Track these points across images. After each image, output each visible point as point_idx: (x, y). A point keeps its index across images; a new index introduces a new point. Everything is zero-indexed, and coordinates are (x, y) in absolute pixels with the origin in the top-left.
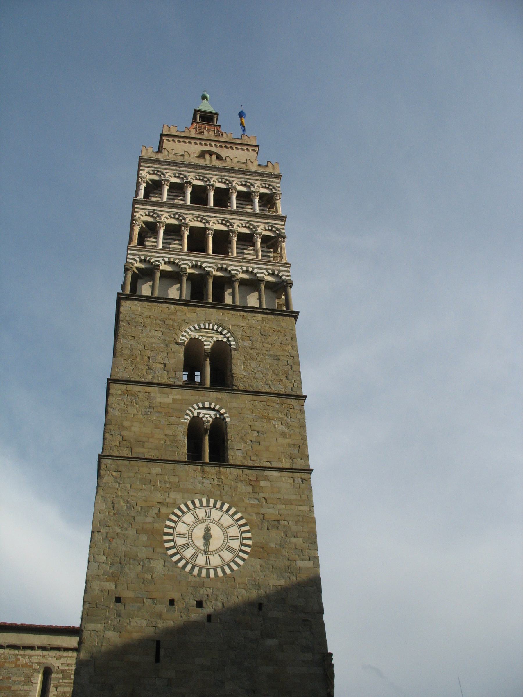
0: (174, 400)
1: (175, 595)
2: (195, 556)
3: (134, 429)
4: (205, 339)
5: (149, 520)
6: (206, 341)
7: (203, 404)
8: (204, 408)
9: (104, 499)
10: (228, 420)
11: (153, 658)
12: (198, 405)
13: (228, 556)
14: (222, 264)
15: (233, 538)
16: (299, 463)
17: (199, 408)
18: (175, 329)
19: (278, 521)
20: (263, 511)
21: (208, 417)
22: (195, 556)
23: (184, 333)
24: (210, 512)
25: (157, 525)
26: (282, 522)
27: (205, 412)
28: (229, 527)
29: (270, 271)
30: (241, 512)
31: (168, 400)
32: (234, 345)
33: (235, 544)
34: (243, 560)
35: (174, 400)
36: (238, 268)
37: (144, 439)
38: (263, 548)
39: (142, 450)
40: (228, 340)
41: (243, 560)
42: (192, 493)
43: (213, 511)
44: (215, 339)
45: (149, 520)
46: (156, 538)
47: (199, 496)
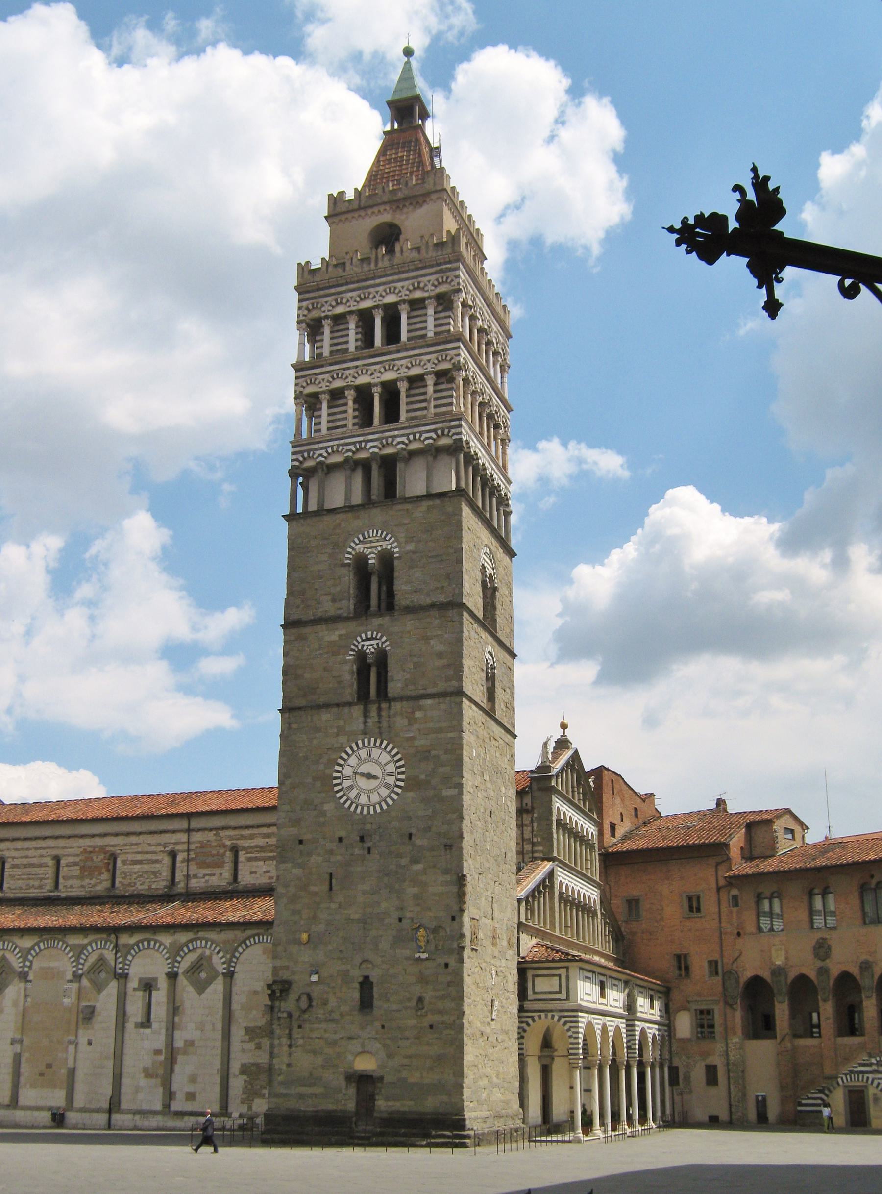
1: (342, 834)
2: (358, 796)
3: (307, 676)
4: (370, 550)
5: (321, 767)
6: (370, 554)
7: (366, 635)
8: (367, 639)
11: (326, 887)
12: (361, 637)
15: (390, 774)
17: (363, 640)
21: (370, 647)
22: (358, 796)
23: (349, 550)
24: (371, 751)
25: (328, 771)
26: (433, 753)
27: (368, 643)
28: (386, 764)
31: (334, 637)
32: (397, 552)
34: (397, 794)
35: (340, 636)
40: (392, 547)
42: (352, 737)
45: (321, 767)
46: (327, 782)
47: (362, 736)
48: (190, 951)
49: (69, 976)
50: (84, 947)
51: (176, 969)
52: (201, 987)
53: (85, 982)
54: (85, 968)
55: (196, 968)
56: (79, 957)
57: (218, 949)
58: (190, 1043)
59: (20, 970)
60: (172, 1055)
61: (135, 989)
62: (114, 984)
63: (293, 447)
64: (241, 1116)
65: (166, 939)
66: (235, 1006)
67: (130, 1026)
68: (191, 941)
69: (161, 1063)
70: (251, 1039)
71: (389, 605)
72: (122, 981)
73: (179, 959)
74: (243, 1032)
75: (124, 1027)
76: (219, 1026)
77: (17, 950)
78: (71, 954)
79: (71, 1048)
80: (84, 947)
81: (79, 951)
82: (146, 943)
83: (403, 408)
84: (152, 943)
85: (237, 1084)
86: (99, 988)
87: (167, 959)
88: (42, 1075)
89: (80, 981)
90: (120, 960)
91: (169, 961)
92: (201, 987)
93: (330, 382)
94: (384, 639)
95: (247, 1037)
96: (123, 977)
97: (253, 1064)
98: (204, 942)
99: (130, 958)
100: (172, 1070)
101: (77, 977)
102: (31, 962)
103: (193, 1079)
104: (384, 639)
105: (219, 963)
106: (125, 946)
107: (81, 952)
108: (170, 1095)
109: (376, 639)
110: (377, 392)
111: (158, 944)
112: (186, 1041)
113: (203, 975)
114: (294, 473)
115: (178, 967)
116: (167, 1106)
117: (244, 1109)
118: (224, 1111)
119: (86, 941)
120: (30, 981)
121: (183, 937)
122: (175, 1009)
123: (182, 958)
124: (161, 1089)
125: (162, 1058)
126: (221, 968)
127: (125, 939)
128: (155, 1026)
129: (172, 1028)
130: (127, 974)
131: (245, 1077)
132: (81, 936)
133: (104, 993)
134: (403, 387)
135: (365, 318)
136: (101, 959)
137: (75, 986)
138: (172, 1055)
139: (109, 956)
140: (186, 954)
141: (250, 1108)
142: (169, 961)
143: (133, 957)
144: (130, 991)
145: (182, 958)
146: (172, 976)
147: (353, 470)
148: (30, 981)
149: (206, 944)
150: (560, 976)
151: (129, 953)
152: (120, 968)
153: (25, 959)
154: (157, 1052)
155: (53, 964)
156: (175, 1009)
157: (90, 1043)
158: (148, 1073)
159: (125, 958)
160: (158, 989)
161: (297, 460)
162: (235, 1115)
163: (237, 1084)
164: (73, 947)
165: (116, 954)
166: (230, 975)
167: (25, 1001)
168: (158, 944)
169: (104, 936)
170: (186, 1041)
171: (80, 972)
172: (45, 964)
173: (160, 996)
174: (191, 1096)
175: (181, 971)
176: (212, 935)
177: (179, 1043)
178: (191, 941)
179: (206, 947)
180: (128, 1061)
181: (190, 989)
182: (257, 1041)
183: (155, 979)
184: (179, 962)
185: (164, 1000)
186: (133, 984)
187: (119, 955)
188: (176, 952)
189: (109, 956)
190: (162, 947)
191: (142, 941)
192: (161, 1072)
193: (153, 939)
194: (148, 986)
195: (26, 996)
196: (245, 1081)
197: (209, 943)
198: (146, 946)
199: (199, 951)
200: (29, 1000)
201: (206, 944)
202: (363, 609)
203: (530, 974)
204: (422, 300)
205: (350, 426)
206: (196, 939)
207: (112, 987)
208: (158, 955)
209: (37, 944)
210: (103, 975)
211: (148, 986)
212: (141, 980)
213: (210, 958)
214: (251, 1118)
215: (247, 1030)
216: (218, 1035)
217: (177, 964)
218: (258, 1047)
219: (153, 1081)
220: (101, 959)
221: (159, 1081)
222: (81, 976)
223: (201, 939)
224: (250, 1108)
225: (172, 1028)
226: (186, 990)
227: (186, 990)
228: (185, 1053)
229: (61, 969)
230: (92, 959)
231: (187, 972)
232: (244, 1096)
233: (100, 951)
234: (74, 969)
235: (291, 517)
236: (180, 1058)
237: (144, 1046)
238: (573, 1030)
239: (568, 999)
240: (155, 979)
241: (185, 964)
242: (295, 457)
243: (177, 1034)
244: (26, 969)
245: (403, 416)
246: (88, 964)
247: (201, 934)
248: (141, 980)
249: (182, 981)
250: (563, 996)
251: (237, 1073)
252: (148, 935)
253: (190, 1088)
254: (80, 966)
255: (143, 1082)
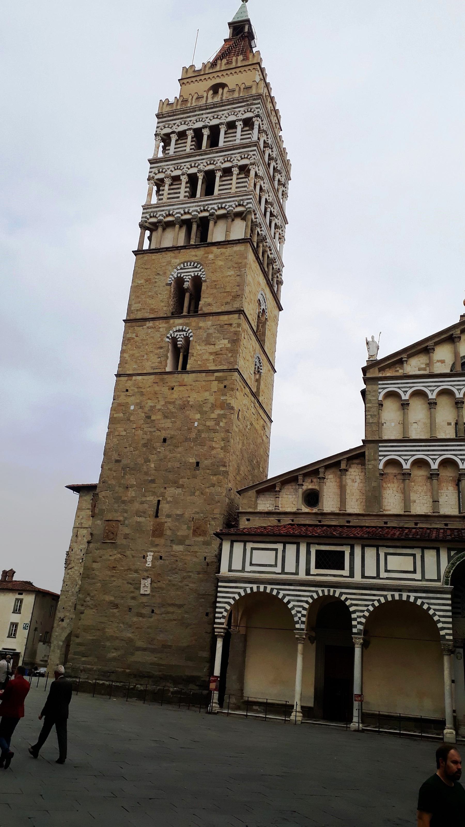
63: (144, 209)
71: (194, 311)
83: (217, 188)
93: (172, 171)
94: (190, 331)
104: (190, 331)
109: (185, 331)
110: (201, 177)
114: (143, 227)
134: (218, 174)
135: (198, 133)
147: (181, 227)
161: (146, 217)
202: (177, 312)
204: (234, 122)
205: (182, 197)
235: (138, 253)
242: (144, 215)
245: (216, 192)
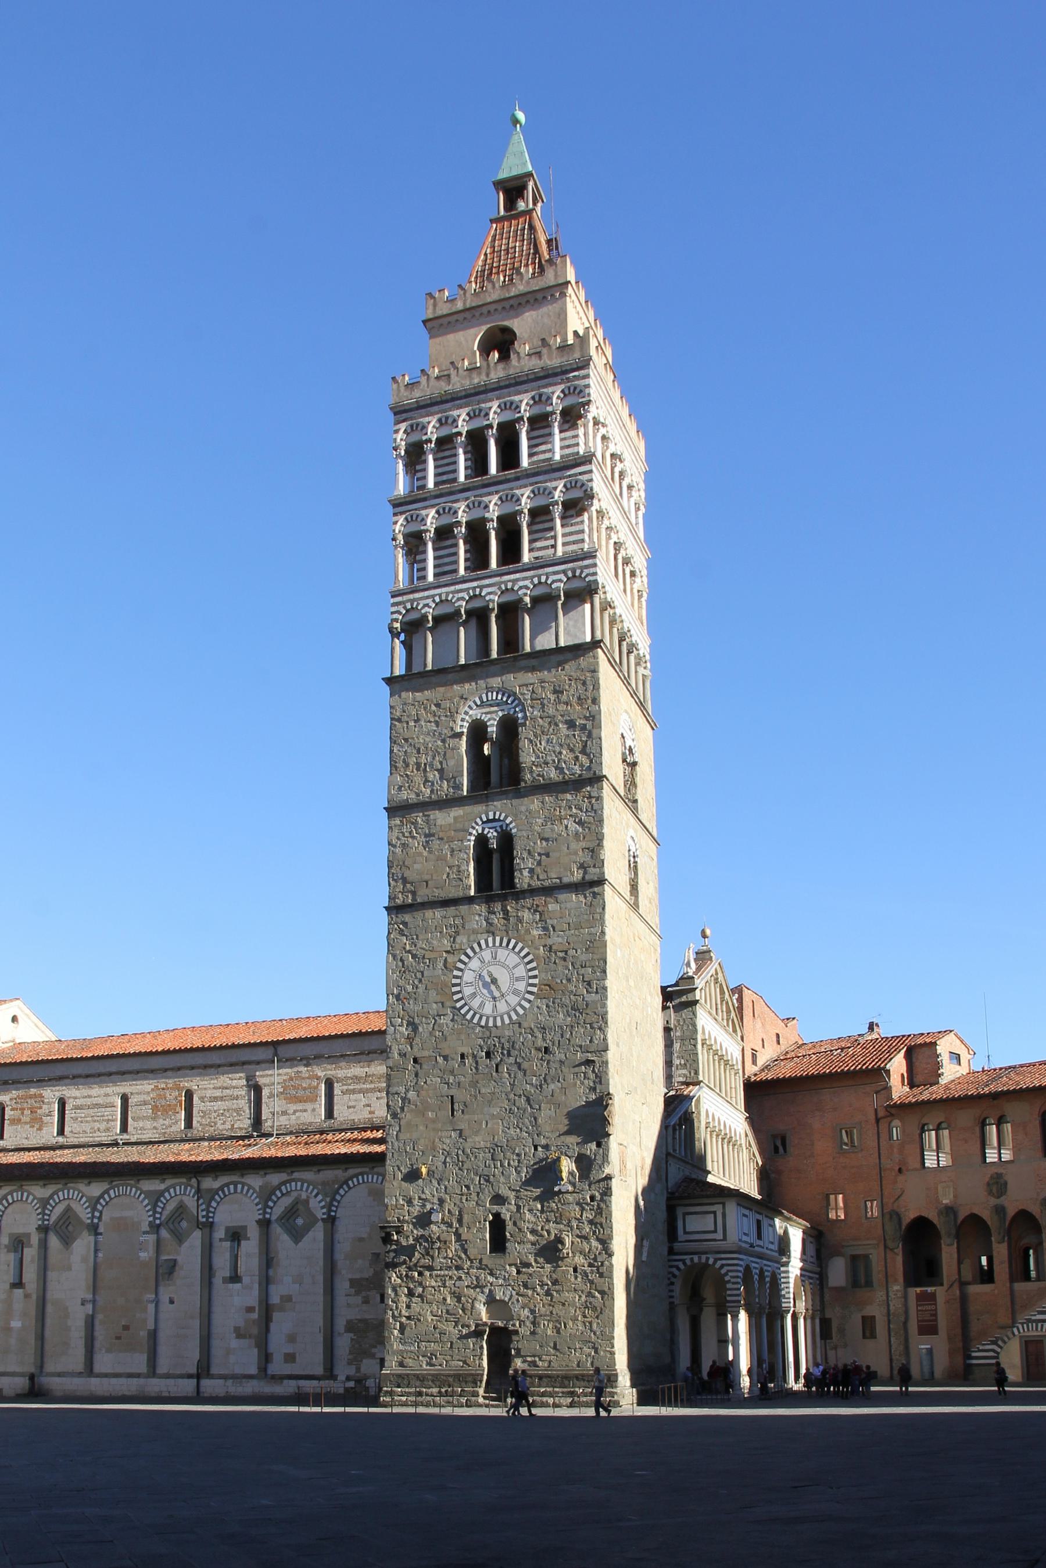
0: (455, 818)
1: (466, 1050)
2: (482, 1005)
4: (489, 716)
6: (489, 720)
7: (487, 816)
9: (394, 956)
10: (514, 831)
12: (481, 819)
13: (513, 1000)
14: (506, 583)
16: (592, 874)
18: (452, 715)
19: (566, 952)
20: (549, 942)
22: (482, 1005)
23: (464, 716)
26: (571, 952)
27: (490, 825)
28: (514, 968)
29: (570, 574)
30: (528, 947)
33: (521, 986)
34: (529, 1001)
36: (527, 583)
37: (426, 877)
38: (549, 986)
39: (427, 891)
41: (529, 1001)
43: (500, 951)
44: (500, 714)
47: (485, 936)
48: (283, 1195)
49: (145, 1227)
50: (161, 1193)
51: (268, 1216)
52: (297, 1235)
53: (164, 1233)
54: (163, 1218)
55: (291, 1213)
56: (155, 1205)
57: (316, 1191)
58: (287, 1299)
59: (89, 1221)
60: (267, 1311)
61: (221, 1240)
62: (197, 1234)
64: (348, 1379)
65: (255, 1181)
66: (339, 1256)
67: (217, 1281)
68: (284, 1183)
69: (254, 1321)
70: (357, 1293)
72: (207, 1230)
73: (271, 1204)
74: (347, 1284)
75: (210, 1283)
76: (320, 1278)
77: (84, 1199)
78: (146, 1201)
79: (151, 1307)
80: (161, 1193)
81: (156, 1198)
82: (232, 1187)
84: (239, 1186)
85: (343, 1343)
86: (180, 1238)
87: (257, 1205)
88: (118, 1338)
89: (157, 1233)
90: (204, 1207)
91: (260, 1206)
92: (297, 1235)
95: (353, 1290)
96: (209, 1226)
97: (360, 1320)
98: (299, 1184)
99: (214, 1204)
100: (267, 1330)
101: (155, 1228)
102: (101, 1212)
103: (292, 1339)
105: (317, 1206)
106: (209, 1190)
107: (158, 1200)
108: (266, 1358)
111: (246, 1188)
112: (282, 1297)
113: (300, 1221)
115: (270, 1214)
116: (263, 1372)
117: (351, 1371)
118: (330, 1374)
119: (162, 1187)
120: (101, 1234)
121: (275, 1178)
122: (268, 1261)
123: (275, 1203)
124: (256, 1350)
125: (255, 1316)
126: (320, 1214)
127: (209, 1183)
128: (246, 1280)
129: (266, 1282)
130: (212, 1223)
131: (352, 1335)
132: (157, 1182)
133: (186, 1244)
136: (181, 1208)
137: (152, 1238)
138: (267, 1311)
139: (190, 1202)
140: (279, 1198)
141: (358, 1370)
142: (260, 1206)
143: (218, 1203)
144: (216, 1243)
145: (275, 1203)
146: (265, 1224)
148: (101, 1234)
149: (302, 1186)
150: (715, 1213)
151: (213, 1198)
152: (203, 1217)
153: (94, 1209)
154: (250, 1310)
155: (127, 1214)
156: (268, 1261)
157: (172, 1302)
158: (239, 1334)
159: (209, 1205)
160: (248, 1239)
162: (342, 1377)
163: (343, 1343)
164: (148, 1194)
165: (198, 1200)
166: (331, 1221)
167: (96, 1256)
168: (246, 1188)
169: (184, 1180)
170: (282, 1297)
171: (158, 1222)
172: (117, 1214)
173: (250, 1247)
174: (290, 1358)
175: (274, 1218)
176: (308, 1175)
177: (275, 1300)
178: (284, 1183)
179: (301, 1190)
180: (217, 1319)
181: (285, 1237)
182: (364, 1294)
183: (245, 1228)
184: (271, 1208)
185: (257, 1251)
186: (220, 1233)
187: (201, 1201)
188: (267, 1196)
189: (190, 1202)
190: (251, 1191)
191: (227, 1185)
192: (255, 1331)
193: (240, 1183)
194: (236, 1236)
195: (96, 1251)
196: (352, 1339)
197: (306, 1185)
198: (232, 1191)
199: (294, 1194)
200: (100, 1255)
201: (302, 1186)
203: (680, 1211)
206: (289, 1181)
207: (196, 1238)
208: (248, 1200)
209: (107, 1192)
210: (184, 1224)
211: (236, 1236)
212: (227, 1229)
213: (307, 1201)
214: (359, 1381)
215: (353, 1282)
216: (320, 1289)
217: (268, 1210)
218: (366, 1301)
219: (245, 1342)
220: (181, 1208)
221: (253, 1341)
222: (159, 1226)
223: (295, 1180)
224: (358, 1370)
225: (266, 1282)
226: (282, 1239)
227: (282, 1239)
228: (282, 1309)
229: (136, 1220)
230: (171, 1207)
231: (280, 1219)
232: (351, 1357)
233: (179, 1197)
234: (151, 1219)
236: (276, 1316)
237: (235, 1303)
238: (730, 1274)
239: (725, 1238)
240: (245, 1228)
241: (278, 1211)
243: (273, 1288)
244: (96, 1221)
246: (166, 1213)
247: (296, 1175)
248: (227, 1229)
249: (277, 1229)
250: (719, 1235)
251: (342, 1331)
252: (235, 1178)
253: (290, 1350)
254: (158, 1216)
255: (234, 1343)
